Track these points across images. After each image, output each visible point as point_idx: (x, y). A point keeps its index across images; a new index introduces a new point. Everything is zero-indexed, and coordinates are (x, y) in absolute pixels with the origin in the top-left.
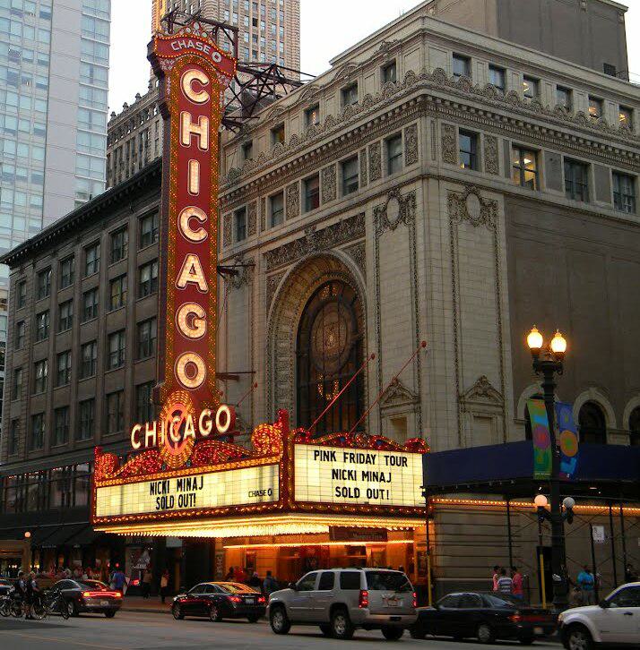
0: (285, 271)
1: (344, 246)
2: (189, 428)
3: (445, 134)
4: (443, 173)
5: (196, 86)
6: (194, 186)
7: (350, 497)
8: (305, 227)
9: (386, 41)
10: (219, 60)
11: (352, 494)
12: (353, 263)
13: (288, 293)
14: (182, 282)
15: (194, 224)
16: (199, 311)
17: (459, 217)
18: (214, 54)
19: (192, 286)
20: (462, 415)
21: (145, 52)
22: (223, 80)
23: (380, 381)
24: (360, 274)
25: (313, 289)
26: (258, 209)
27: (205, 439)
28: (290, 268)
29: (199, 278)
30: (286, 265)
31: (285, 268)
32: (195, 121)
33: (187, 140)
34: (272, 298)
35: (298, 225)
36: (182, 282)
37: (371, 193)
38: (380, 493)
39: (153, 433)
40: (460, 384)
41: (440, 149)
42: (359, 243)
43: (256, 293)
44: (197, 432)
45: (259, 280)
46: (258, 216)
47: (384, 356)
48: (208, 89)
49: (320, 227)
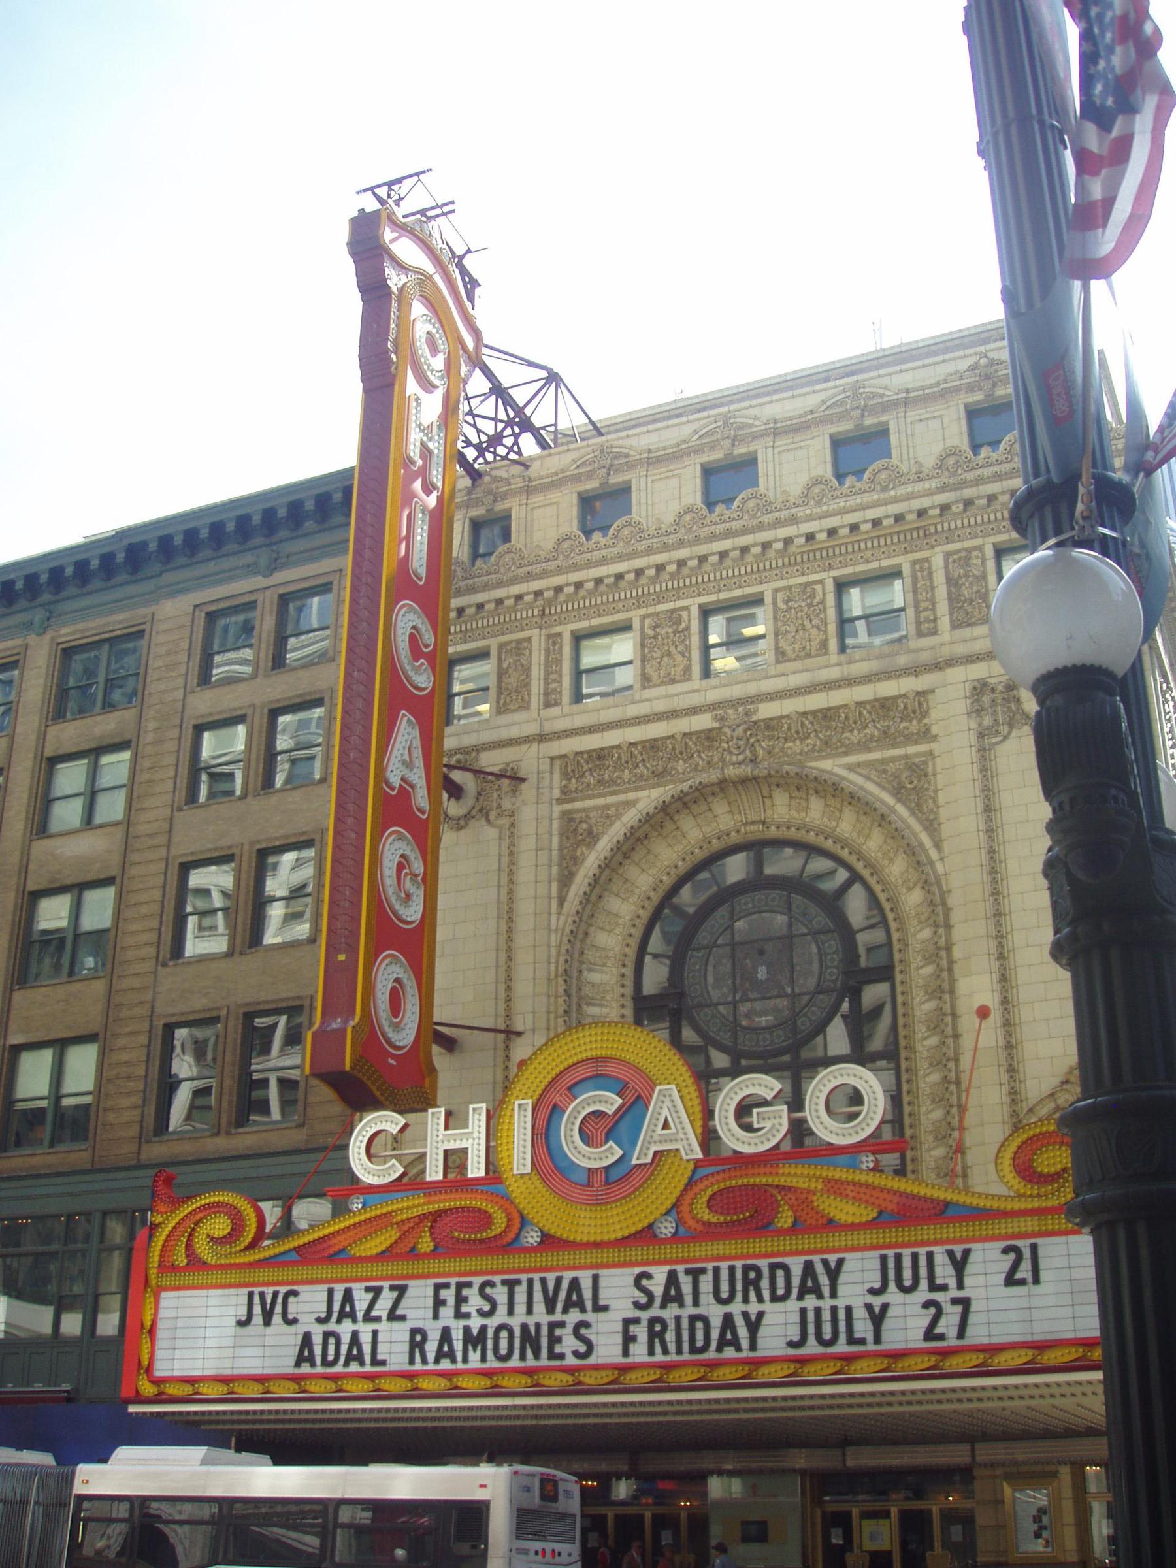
0: (633, 803)
1: (852, 759)
2: (666, 1126)
8: (713, 707)
9: (991, 355)
12: (890, 800)
13: (626, 856)
19: (405, 793)
21: (343, 234)
23: (1012, 1070)
24: (912, 821)
25: (700, 855)
26: (537, 659)
27: (740, 1161)
28: (649, 798)
29: (418, 777)
30: (636, 789)
31: (631, 796)
34: (576, 861)
35: (695, 700)
37: (961, 650)
39: (472, 1139)
42: (907, 756)
43: (527, 845)
44: (709, 1137)
45: (536, 815)
46: (536, 672)
47: (1025, 1014)
49: (767, 710)
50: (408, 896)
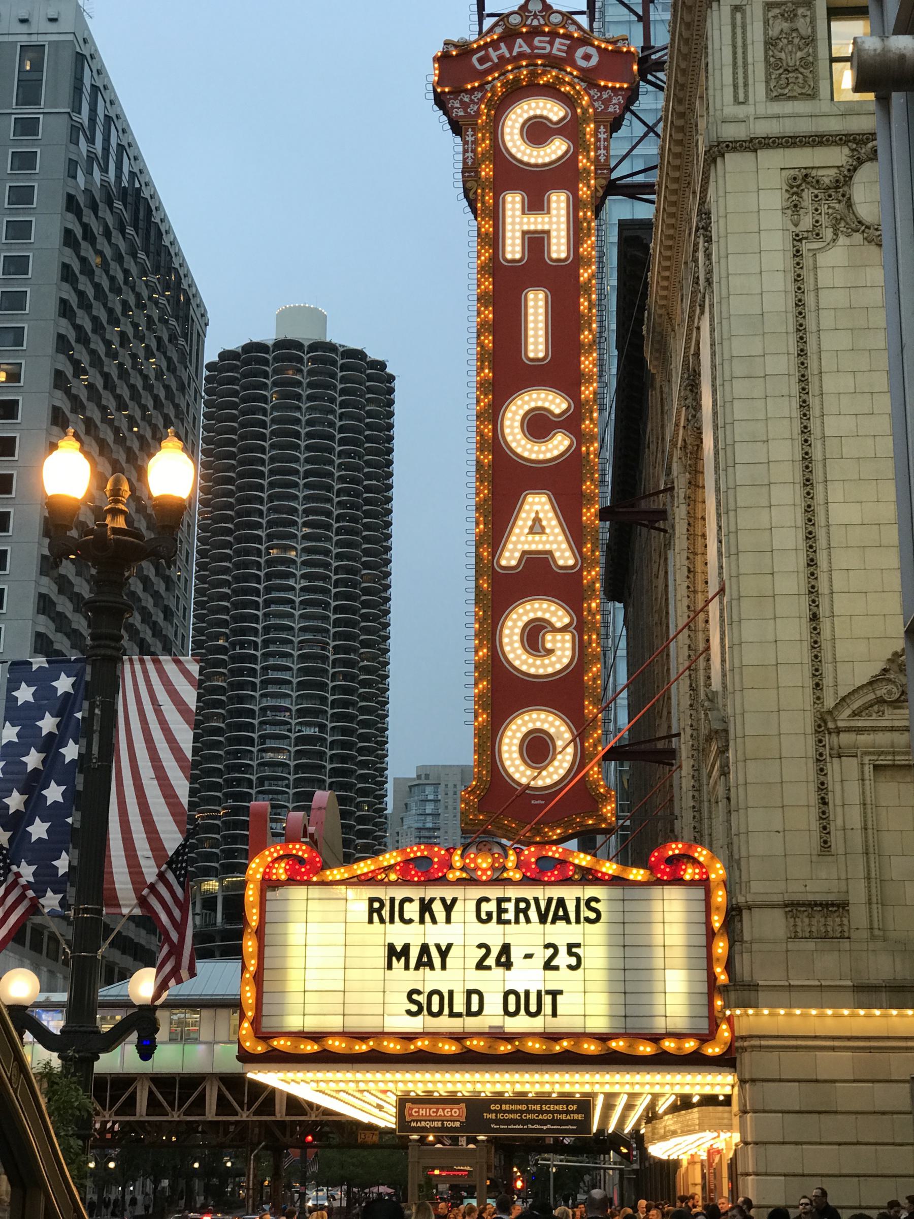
3: (781, 25)
4: (762, 129)
5: (537, 132)
6: (536, 344)
7: (452, 1014)
10: (594, 61)
11: (459, 1007)
14: (510, 557)
16: (556, 614)
17: (828, 234)
18: (580, 52)
20: (834, 767)
32: (536, 205)
33: (513, 249)
36: (510, 557)
38: (548, 999)
40: (828, 681)
41: (758, 71)
48: (570, 129)
50: (550, 652)
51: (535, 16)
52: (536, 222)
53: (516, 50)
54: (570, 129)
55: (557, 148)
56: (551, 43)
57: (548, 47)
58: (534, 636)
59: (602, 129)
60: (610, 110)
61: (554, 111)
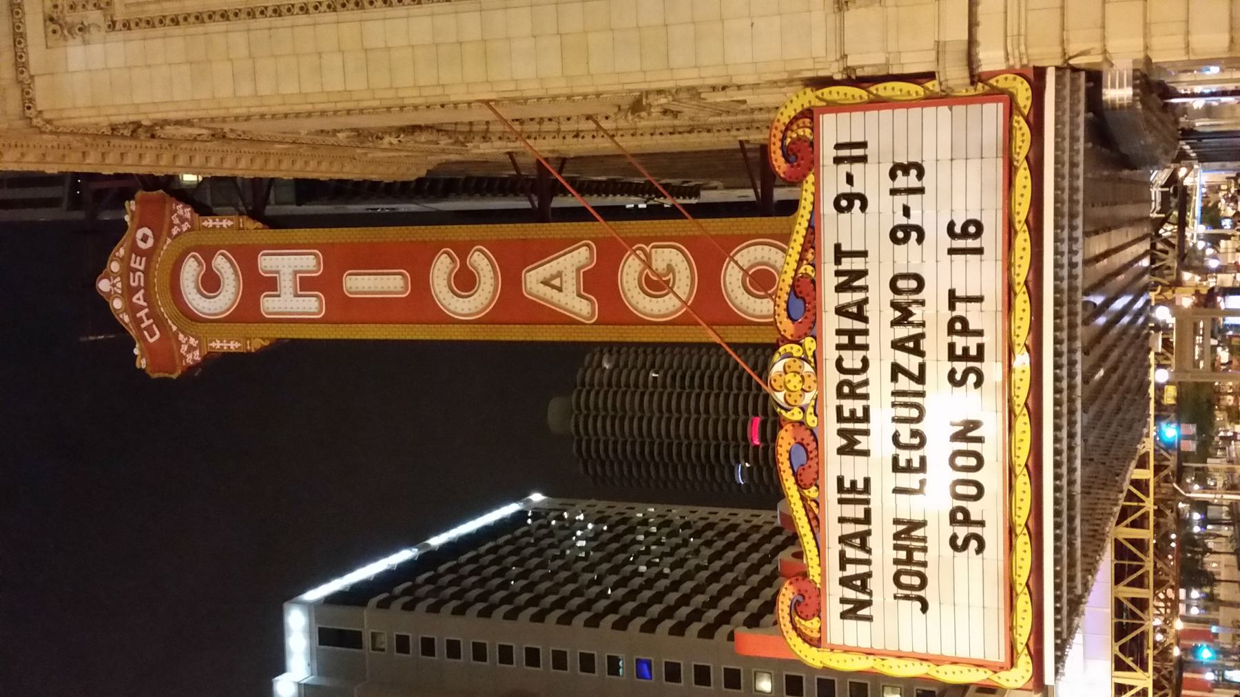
5: (211, 283)
6: (391, 284)
15: (465, 282)
18: (141, 245)
22: (183, 220)
32: (271, 284)
33: (311, 305)
48: (208, 254)
50: (670, 269)
51: (114, 285)
52: (286, 284)
53: (142, 303)
54: (208, 254)
55: (221, 264)
56: (135, 271)
57: (138, 273)
58: (656, 285)
59: (205, 223)
60: (188, 215)
61: (191, 270)
